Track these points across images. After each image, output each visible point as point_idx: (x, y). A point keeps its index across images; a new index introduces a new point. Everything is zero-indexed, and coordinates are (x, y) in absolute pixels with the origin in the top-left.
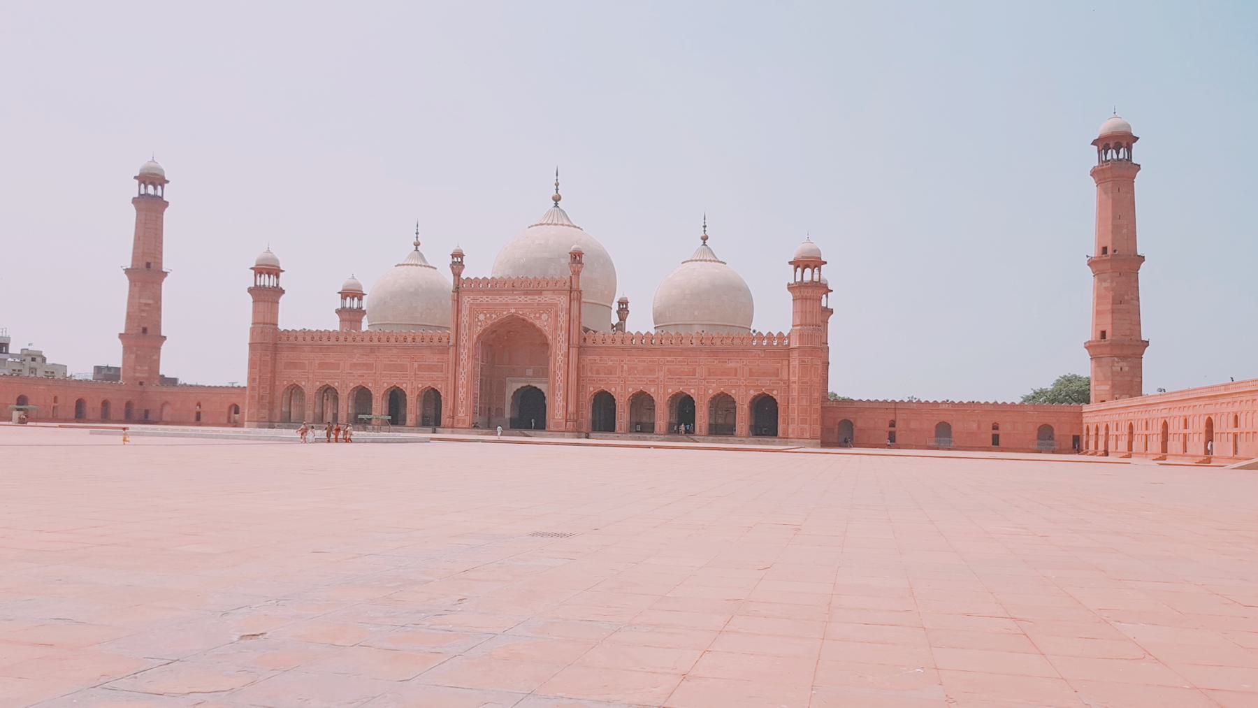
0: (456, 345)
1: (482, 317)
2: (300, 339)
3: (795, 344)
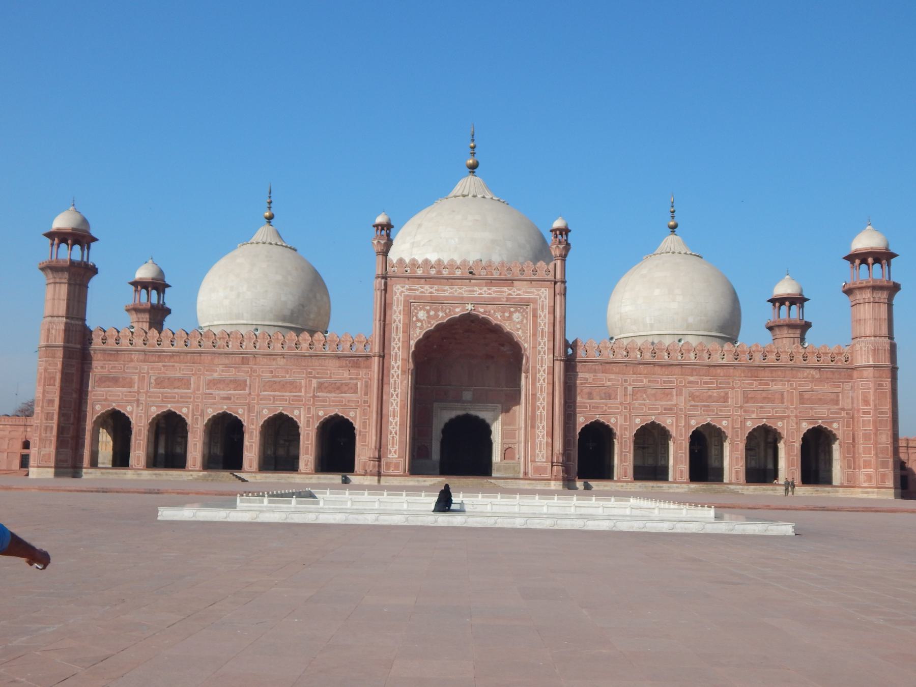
1: (422, 315)
2: (125, 342)
3: (863, 357)
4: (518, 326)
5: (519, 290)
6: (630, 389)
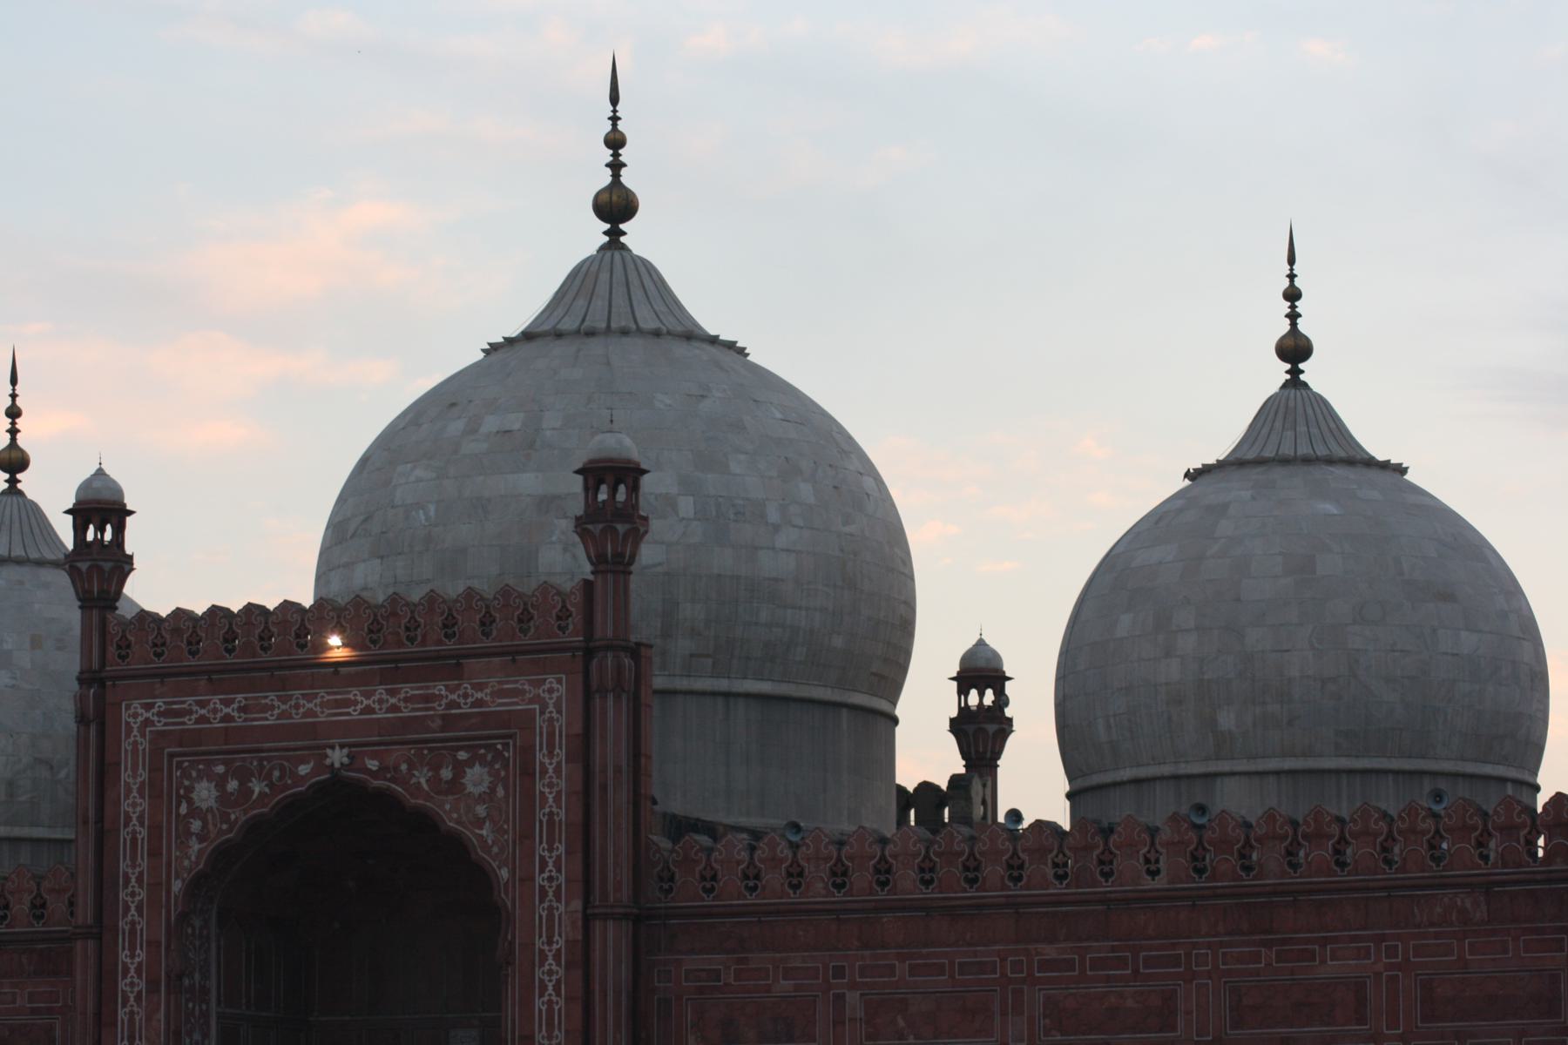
0: (101, 930)
1: (205, 793)
4: (481, 810)
5: (479, 687)
6: (853, 997)
